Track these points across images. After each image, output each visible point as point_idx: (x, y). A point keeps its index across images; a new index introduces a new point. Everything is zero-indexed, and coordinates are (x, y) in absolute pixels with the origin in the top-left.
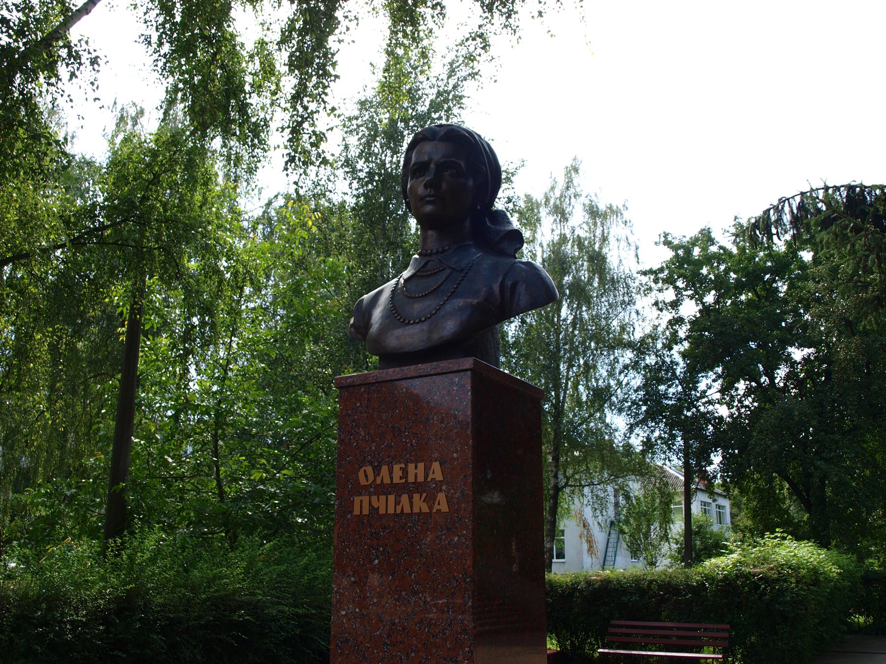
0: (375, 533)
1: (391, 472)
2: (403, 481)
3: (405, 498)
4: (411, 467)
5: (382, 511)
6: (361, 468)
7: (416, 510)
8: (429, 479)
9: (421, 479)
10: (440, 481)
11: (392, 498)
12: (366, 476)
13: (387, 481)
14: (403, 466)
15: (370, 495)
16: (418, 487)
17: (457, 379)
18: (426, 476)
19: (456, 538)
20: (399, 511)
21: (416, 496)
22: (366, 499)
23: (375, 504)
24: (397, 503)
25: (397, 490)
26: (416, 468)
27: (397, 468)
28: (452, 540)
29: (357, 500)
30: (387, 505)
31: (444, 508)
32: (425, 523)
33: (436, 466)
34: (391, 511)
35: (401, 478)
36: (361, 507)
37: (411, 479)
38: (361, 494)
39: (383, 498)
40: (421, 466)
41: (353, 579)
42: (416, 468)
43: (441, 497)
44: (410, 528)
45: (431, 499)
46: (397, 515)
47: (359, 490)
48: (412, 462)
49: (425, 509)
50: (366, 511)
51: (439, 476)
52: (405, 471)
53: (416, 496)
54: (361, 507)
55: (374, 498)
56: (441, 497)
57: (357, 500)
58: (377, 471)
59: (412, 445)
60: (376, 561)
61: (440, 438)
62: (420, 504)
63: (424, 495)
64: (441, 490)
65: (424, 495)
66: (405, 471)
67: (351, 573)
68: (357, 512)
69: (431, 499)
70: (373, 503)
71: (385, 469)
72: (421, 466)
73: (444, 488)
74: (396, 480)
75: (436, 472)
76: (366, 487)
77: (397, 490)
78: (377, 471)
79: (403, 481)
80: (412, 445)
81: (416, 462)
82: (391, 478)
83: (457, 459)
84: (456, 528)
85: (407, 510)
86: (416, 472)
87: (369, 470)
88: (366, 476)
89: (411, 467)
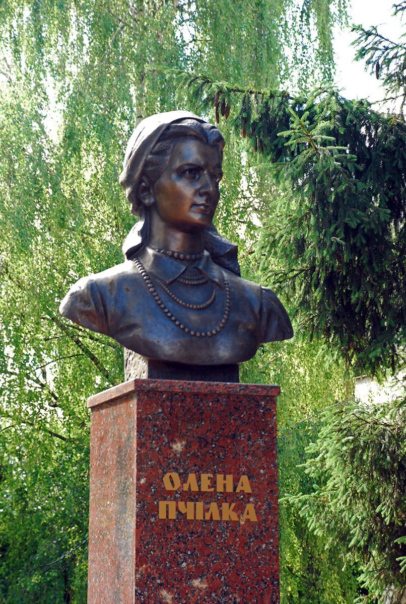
0: (182, 537)
1: (199, 479)
2: (212, 490)
3: (214, 506)
4: (220, 477)
5: (190, 517)
6: (165, 473)
7: (225, 518)
8: (238, 491)
9: (230, 489)
10: (248, 494)
11: (200, 505)
12: (172, 482)
13: (195, 488)
14: (211, 476)
15: (176, 499)
16: (226, 497)
17: (263, 403)
18: (235, 488)
19: (264, 546)
20: (208, 518)
21: (225, 505)
22: (172, 505)
23: (183, 509)
24: (206, 510)
25: (198, 496)
26: (225, 479)
27: (205, 477)
28: (260, 547)
29: (162, 505)
30: (194, 511)
31: (253, 518)
32: (233, 530)
33: (244, 479)
34: (200, 517)
35: (209, 487)
36: (167, 512)
37: (220, 489)
38: (165, 499)
39: (191, 504)
40: (230, 478)
41: (159, 581)
42: (225, 479)
43: (250, 507)
44: (219, 533)
45: (240, 509)
46: (206, 522)
47: (164, 495)
48: (219, 473)
49: (234, 517)
50: (173, 515)
51: (248, 489)
52: (214, 483)
53: (225, 505)
54: (167, 512)
55: (181, 505)
56: (250, 507)
57: (162, 505)
58: (184, 478)
59: (219, 457)
60: (184, 564)
61: (248, 454)
62: (228, 512)
63: (233, 505)
64: (249, 502)
65: (233, 505)
66: (214, 483)
67: (157, 575)
68: (162, 515)
69: (240, 509)
70: (180, 509)
71: (192, 477)
72: (230, 478)
73: (251, 499)
74: (204, 488)
75: (245, 484)
76: (170, 492)
77: (198, 496)
78: (184, 478)
79: (212, 490)
80: (219, 457)
81: (225, 473)
82: (199, 486)
83: (264, 475)
84: (264, 536)
85: (216, 517)
86: (225, 483)
87: (175, 476)
88: (172, 482)
89: (220, 477)
